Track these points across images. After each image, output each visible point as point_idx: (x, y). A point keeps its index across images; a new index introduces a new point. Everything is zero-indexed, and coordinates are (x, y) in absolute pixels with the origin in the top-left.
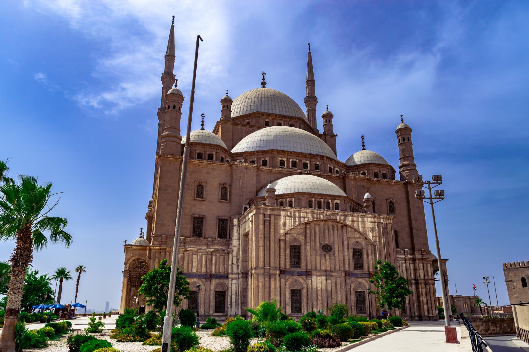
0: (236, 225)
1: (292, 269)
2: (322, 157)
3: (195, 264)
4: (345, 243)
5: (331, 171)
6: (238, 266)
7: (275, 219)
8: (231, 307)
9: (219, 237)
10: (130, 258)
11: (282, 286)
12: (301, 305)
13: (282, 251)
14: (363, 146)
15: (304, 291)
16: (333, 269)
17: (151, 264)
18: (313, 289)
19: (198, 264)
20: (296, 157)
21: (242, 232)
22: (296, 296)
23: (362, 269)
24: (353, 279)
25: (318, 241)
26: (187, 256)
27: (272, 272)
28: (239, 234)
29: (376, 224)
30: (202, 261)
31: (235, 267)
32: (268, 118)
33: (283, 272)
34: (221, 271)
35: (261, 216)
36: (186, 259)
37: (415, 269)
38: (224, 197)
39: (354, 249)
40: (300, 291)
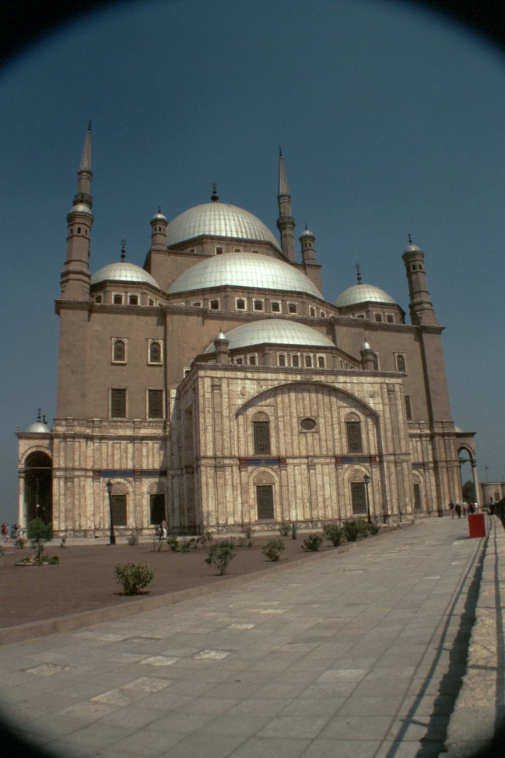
1: (258, 456)
2: (299, 294)
4: (335, 415)
5: (313, 314)
6: (181, 457)
7: (228, 384)
9: (150, 417)
10: (26, 451)
11: (244, 480)
12: (272, 506)
13: (241, 430)
14: (359, 279)
15: (276, 488)
16: (317, 453)
20: (262, 295)
21: (183, 407)
22: (265, 495)
24: (346, 466)
26: (105, 447)
27: (227, 461)
28: (180, 410)
29: (379, 385)
30: (126, 453)
32: (219, 243)
33: (244, 462)
35: (208, 382)
37: (434, 449)
38: (155, 357)
39: (348, 423)
40: (270, 487)
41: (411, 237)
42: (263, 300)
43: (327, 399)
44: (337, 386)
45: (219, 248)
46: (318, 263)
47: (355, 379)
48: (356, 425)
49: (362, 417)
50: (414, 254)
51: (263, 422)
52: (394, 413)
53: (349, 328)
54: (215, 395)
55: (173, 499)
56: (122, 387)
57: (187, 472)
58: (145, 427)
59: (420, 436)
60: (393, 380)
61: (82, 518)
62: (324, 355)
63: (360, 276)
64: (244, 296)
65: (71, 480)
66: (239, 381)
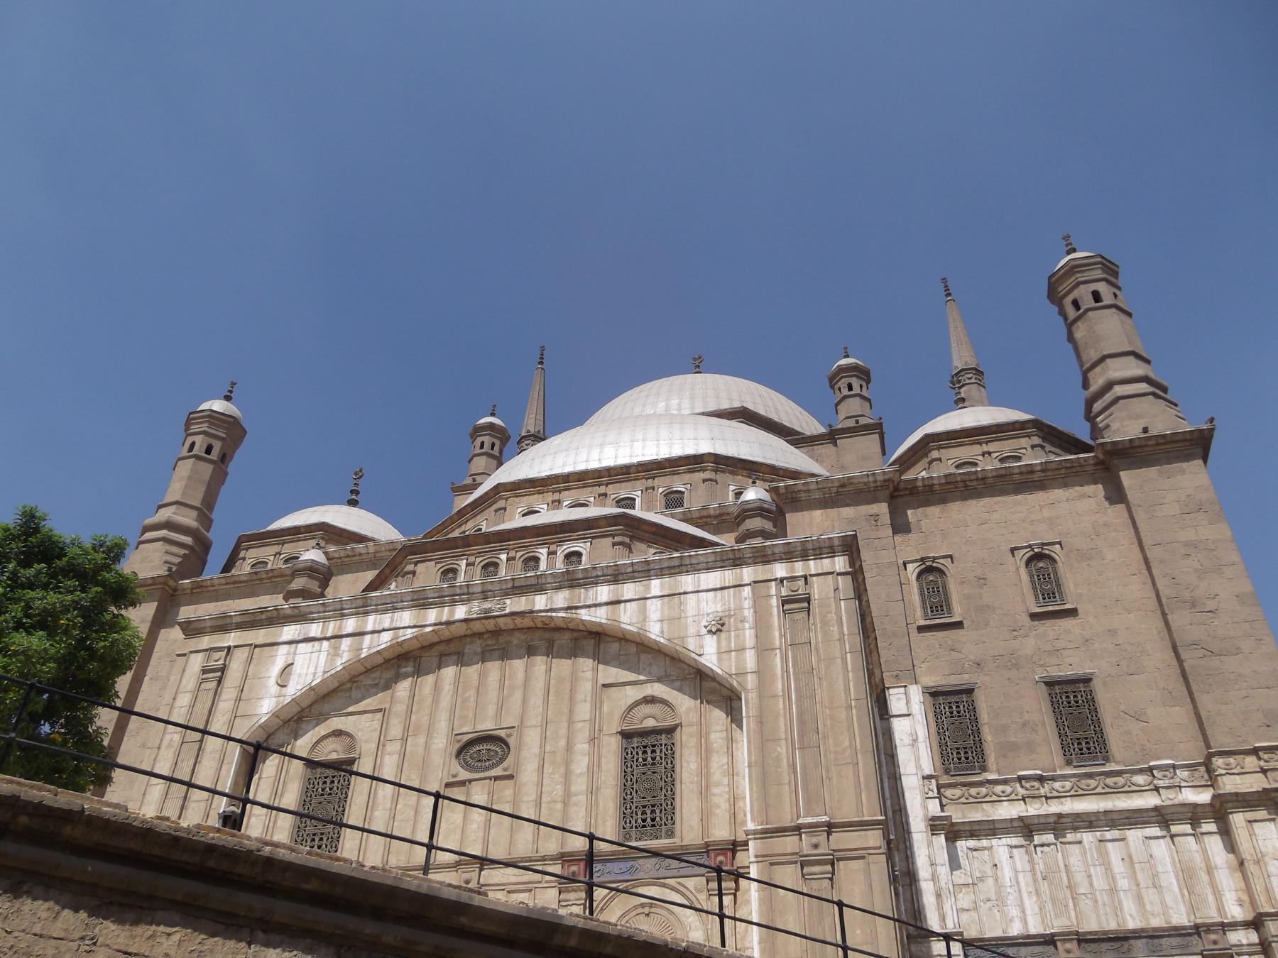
2: (693, 462)
4: (584, 711)
23: (671, 834)
29: (747, 591)
39: (626, 735)
41: (1071, 240)
42: (592, 499)
43: (563, 666)
44: (588, 618)
46: (863, 421)
47: (656, 586)
48: (663, 739)
49: (685, 705)
50: (1072, 269)
52: (805, 675)
53: (833, 512)
59: (1162, 817)
60: (813, 566)
62: (582, 547)
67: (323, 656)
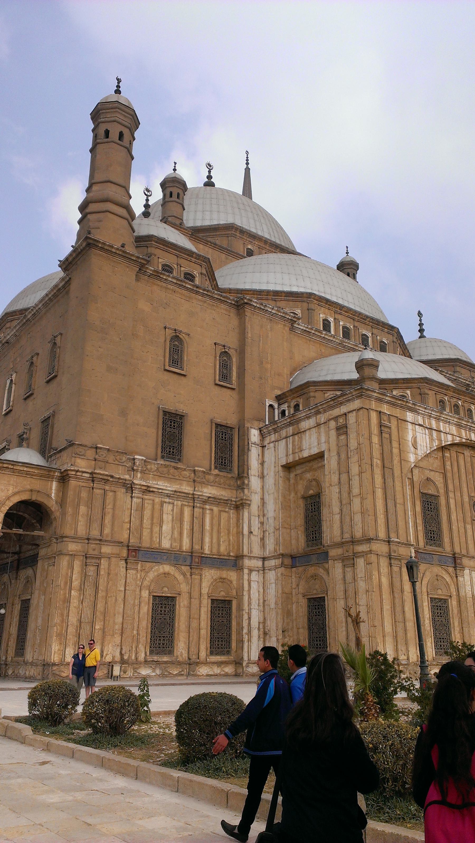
0: (255, 444)
3: (166, 528)
6: (262, 539)
8: (249, 640)
9: (216, 468)
10: (8, 498)
14: (421, 331)
17: (69, 518)
18: (468, 599)
19: (173, 528)
25: (465, 489)
26: (150, 507)
28: (262, 463)
30: (181, 521)
31: (255, 540)
34: (222, 549)
36: (147, 513)
42: (352, 327)
45: (248, 249)
51: (432, 495)
54: (385, 441)
55: (250, 609)
56: (180, 412)
57: (282, 565)
58: (208, 483)
61: (108, 638)
63: (424, 327)
64: (331, 316)
65: (93, 561)
66: (410, 426)
67: (427, 437)
